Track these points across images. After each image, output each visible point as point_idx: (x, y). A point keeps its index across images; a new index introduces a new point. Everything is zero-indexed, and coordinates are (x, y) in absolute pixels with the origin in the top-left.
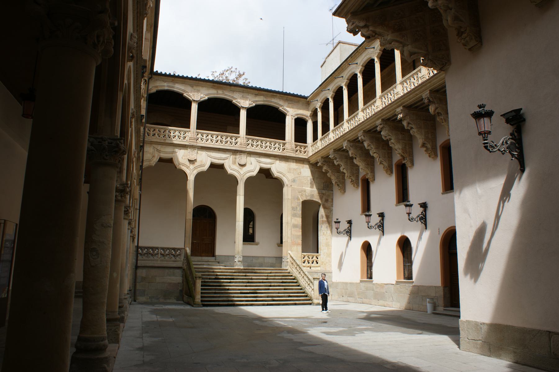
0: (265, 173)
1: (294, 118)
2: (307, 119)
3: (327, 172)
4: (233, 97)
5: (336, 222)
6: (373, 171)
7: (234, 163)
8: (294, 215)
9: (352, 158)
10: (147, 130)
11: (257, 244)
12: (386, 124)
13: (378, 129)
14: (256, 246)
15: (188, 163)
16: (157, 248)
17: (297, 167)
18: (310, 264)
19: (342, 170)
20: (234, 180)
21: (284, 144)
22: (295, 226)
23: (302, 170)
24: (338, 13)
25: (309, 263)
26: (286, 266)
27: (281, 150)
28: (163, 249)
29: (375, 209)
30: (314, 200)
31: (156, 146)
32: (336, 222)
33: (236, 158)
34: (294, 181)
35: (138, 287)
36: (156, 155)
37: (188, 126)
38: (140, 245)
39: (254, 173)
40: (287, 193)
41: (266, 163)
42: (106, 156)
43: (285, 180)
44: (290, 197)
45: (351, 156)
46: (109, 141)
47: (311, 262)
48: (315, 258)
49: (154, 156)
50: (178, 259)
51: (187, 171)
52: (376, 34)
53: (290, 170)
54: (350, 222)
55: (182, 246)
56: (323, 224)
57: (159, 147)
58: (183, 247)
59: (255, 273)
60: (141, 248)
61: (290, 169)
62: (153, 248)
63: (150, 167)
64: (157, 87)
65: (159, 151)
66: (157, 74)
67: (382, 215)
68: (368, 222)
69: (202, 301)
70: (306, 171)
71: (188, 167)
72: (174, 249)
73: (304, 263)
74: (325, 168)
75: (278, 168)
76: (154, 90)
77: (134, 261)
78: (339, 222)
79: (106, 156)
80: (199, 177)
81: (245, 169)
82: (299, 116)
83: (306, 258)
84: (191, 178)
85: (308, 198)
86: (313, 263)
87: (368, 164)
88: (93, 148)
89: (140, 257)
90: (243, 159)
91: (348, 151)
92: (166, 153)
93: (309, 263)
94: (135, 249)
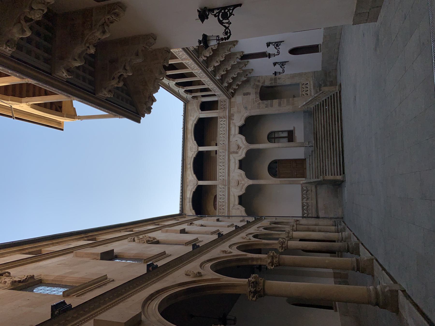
0: (242, 130)
1: (201, 112)
2: (200, 102)
3: (238, 85)
4: (192, 157)
5: (275, 75)
6: (235, 54)
7: (237, 153)
8: (272, 106)
9: (227, 71)
10: (220, 214)
11: (294, 128)
12: (201, 54)
13: (205, 59)
14: (296, 129)
15: (241, 185)
16: (303, 203)
17: (236, 106)
18: (308, 89)
19: (236, 76)
20: (249, 153)
22: (280, 105)
24: (139, 122)
25: (307, 90)
26: (311, 108)
27: (225, 119)
28: (302, 199)
29: (263, 49)
30: (259, 91)
31: (231, 208)
32: (275, 75)
34: (246, 108)
35: (332, 216)
37: (215, 186)
39: (243, 138)
40: (255, 112)
41: (235, 130)
42: (259, 288)
43: (246, 114)
45: (225, 73)
46: (250, 287)
47: (307, 89)
48: (304, 86)
49: (238, 209)
50: (309, 189)
51: (246, 185)
52: (150, 96)
53: (239, 112)
54: (275, 64)
55: (300, 186)
56: (276, 83)
57: (231, 205)
59: (317, 132)
60: (303, 214)
62: (303, 207)
63: (246, 211)
64: (191, 210)
65: (234, 205)
67: (268, 45)
68: (274, 55)
69: (340, 175)
70: (238, 99)
71: (244, 185)
73: (307, 94)
74: (235, 87)
75: (239, 121)
76: (193, 212)
77: (313, 219)
78: (275, 72)
79: (259, 288)
80: (249, 176)
81: (241, 145)
82: (199, 108)
83: (304, 93)
84: (251, 182)
85: (258, 96)
86: (307, 88)
87: (231, 58)
88: (256, 296)
89: (310, 215)
90: (233, 148)
91: (222, 75)
92: (235, 200)
93: (307, 90)
94: (305, 219)
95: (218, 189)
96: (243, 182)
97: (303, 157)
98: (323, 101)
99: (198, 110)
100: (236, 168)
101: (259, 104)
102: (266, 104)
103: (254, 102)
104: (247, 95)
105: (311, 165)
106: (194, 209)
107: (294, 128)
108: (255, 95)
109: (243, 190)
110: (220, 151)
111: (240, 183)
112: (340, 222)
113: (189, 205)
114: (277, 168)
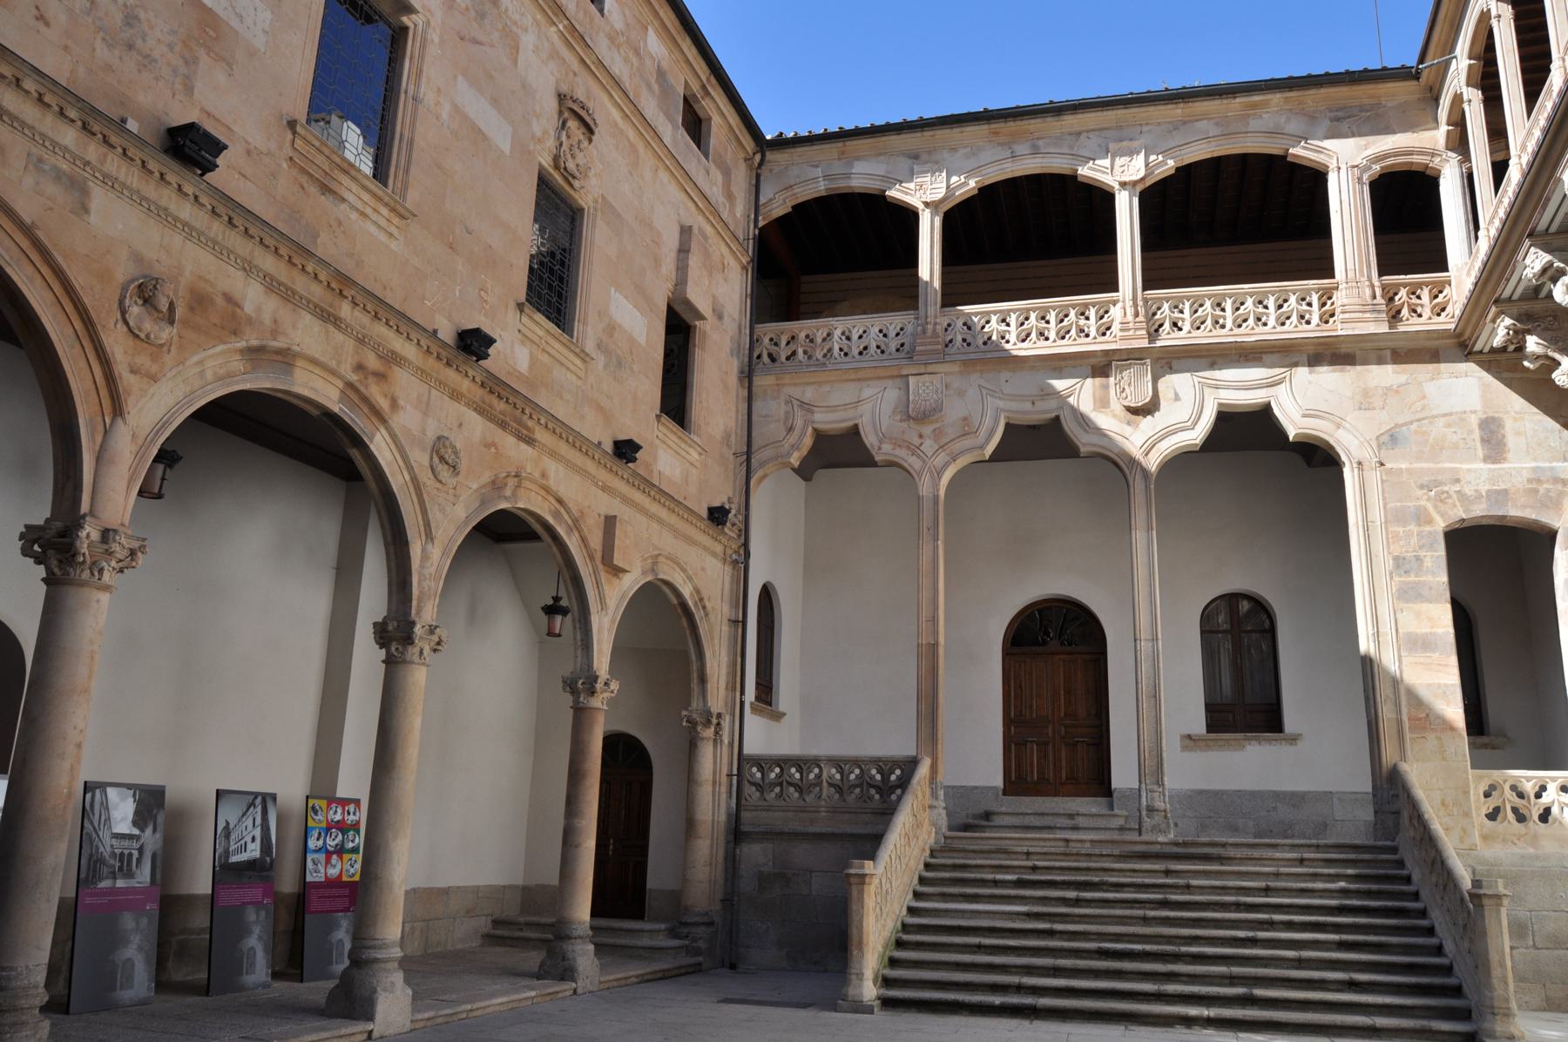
8: (1409, 594)
11: (1293, 739)
16: (816, 762)
17: (1403, 378)
21: (1327, 295)
23: (1430, 388)
25: (1521, 818)
27: (1315, 319)
28: (838, 763)
33: (1106, 387)
34: (1391, 439)
36: (799, 423)
38: (747, 750)
39: (1196, 436)
43: (1350, 443)
44: (1377, 515)
49: (791, 429)
51: (913, 462)
53: (1365, 402)
58: (912, 752)
60: (761, 762)
61: (1366, 393)
62: (802, 763)
65: (807, 407)
66: (781, 143)
71: (915, 450)
72: (877, 762)
75: (1302, 402)
85: (1479, 511)
92: (833, 409)
95: (894, 321)
96: (929, 446)
97: (1116, 782)
98: (1423, 913)
99: (1378, 158)
100: (1014, 405)
101: (1422, 518)
102: (1418, 558)
103: (1438, 484)
104: (1485, 441)
105: (1069, 823)
106: (797, 208)
107: (1293, 739)
108: (1484, 488)
109: (886, 447)
110: (1116, 313)
111: (927, 430)
112: (698, 952)
113: (810, 179)
114: (1057, 648)
